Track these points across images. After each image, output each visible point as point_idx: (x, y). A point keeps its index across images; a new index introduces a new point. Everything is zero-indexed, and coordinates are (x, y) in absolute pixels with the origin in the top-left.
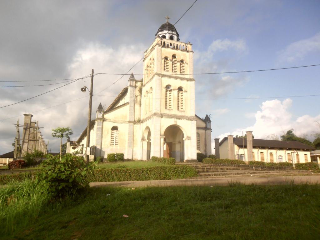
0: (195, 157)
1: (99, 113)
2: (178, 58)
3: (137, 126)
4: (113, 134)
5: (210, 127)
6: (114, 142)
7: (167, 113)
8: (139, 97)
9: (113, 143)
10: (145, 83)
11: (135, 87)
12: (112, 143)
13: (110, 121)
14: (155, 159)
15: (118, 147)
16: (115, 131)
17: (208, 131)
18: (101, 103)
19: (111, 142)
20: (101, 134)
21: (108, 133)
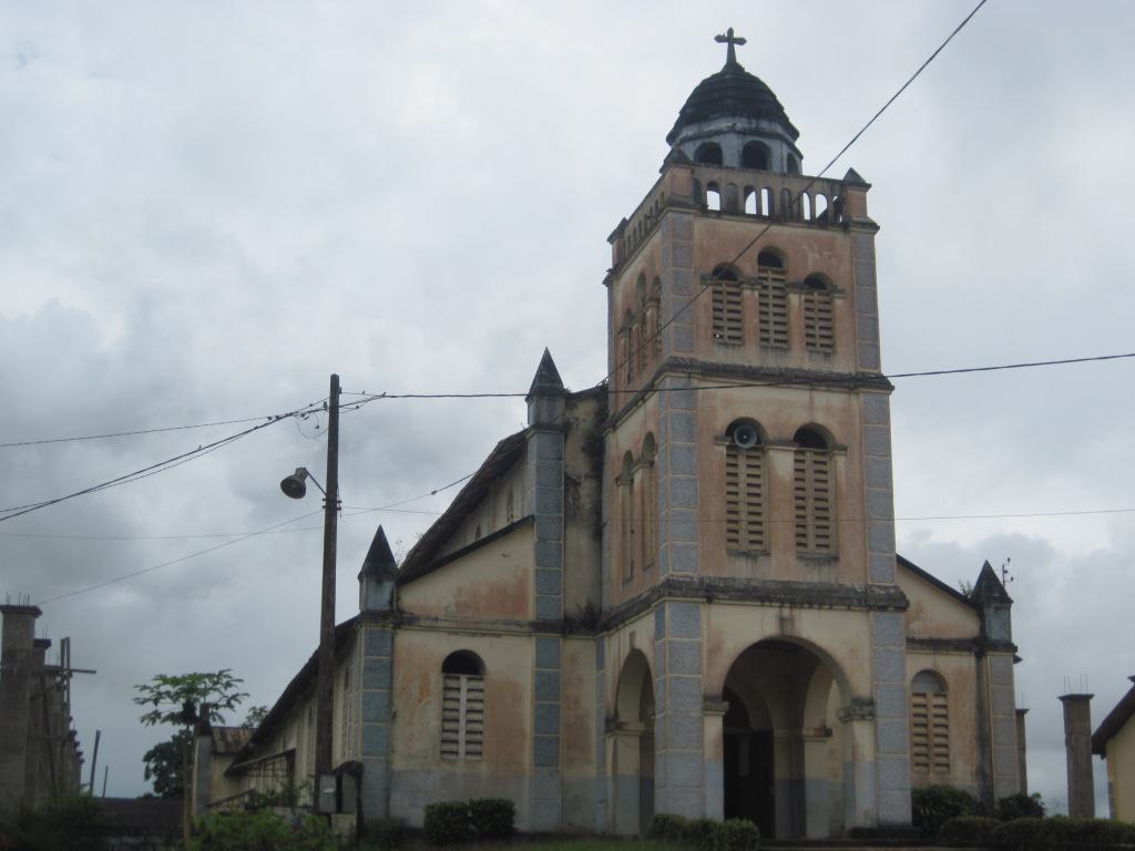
0: (899, 811)
1: (373, 584)
3: (577, 648)
4: (452, 694)
5: (1008, 630)
6: (462, 736)
7: (737, 576)
8: (586, 488)
9: (452, 747)
10: (622, 406)
11: (565, 429)
12: (447, 747)
13: (432, 624)
14: (665, 828)
15: (484, 768)
17: (993, 660)
18: (380, 532)
21: (424, 691)
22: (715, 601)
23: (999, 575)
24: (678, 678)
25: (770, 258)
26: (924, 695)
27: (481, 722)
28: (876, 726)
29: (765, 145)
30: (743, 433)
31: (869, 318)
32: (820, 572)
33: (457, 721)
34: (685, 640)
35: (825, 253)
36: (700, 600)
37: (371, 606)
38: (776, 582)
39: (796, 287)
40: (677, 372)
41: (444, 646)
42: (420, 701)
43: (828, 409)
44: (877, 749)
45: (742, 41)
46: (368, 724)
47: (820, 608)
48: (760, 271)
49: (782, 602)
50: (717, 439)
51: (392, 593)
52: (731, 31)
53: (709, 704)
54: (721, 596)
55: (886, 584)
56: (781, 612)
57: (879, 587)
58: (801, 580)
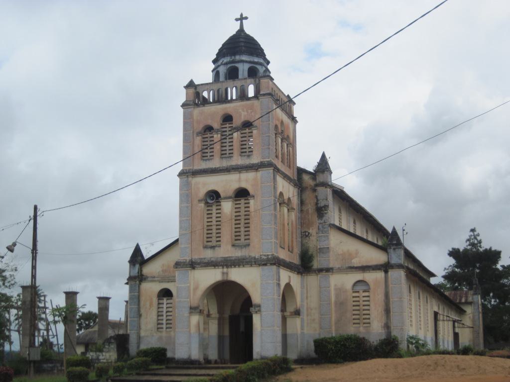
2: (237, 122)
4: (161, 306)
6: (164, 322)
7: (207, 257)
12: (159, 326)
13: (153, 279)
16: (165, 299)
19: (158, 324)
20: (137, 310)
23: (400, 233)
24: (180, 301)
25: (228, 118)
26: (358, 292)
27: (171, 316)
28: (261, 315)
30: (214, 196)
33: (162, 316)
34: (183, 285)
35: (249, 111)
36: (189, 269)
37: (132, 275)
39: (237, 129)
41: (157, 287)
42: (150, 309)
43: (247, 181)
44: (261, 326)
45: (246, 18)
47: (239, 267)
48: (222, 124)
50: (200, 201)
52: (242, 15)
53: (192, 310)
54: (198, 266)
58: (233, 255)
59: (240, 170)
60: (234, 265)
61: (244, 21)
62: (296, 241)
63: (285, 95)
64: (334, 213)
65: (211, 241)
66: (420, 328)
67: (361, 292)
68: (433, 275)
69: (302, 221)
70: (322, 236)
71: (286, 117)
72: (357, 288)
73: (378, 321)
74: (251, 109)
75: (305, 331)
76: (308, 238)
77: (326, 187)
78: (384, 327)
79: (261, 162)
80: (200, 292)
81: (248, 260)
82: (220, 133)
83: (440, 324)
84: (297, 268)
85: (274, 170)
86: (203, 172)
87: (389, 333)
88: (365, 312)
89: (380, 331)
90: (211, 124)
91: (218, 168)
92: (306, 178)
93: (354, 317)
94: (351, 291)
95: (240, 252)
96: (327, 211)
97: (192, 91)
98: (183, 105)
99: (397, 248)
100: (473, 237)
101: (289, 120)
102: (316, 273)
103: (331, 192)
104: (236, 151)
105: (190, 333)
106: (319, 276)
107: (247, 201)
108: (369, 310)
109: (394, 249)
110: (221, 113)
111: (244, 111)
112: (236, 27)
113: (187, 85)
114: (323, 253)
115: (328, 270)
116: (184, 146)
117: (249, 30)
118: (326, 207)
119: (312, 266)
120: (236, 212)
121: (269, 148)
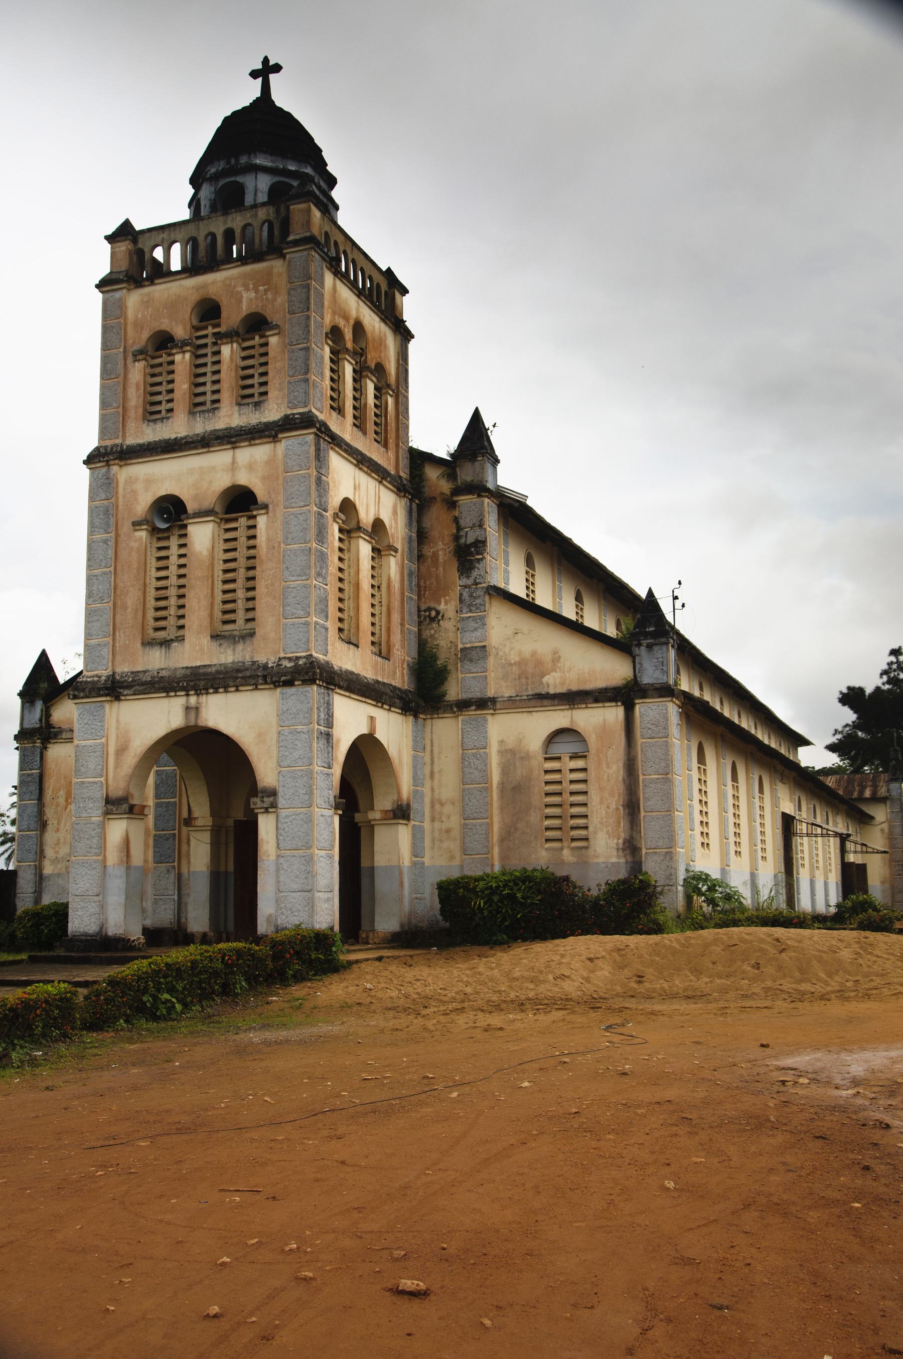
2: (231, 318)
7: (150, 668)
22: (123, 698)
24: (83, 783)
26: (559, 758)
29: (238, 182)
31: (301, 349)
32: (234, 650)
35: (261, 288)
37: (26, 726)
38: (187, 668)
40: (97, 462)
42: (66, 809)
43: (251, 467)
44: (278, 847)
45: (277, 68)
46: (21, 833)
47: (226, 692)
49: (187, 690)
50: (136, 524)
51: (42, 710)
53: (110, 807)
54: (125, 693)
55: (298, 655)
56: (187, 701)
57: (290, 659)
58: (215, 661)
59: (233, 440)
60: (212, 687)
61: (272, 77)
62: (402, 632)
63: (379, 269)
64: (507, 564)
65: (164, 629)
66: (738, 853)
67: (566, 758)
68: (800, 741)
69: (422, 584)
70: (470, 617)
71: (377, 319)
72: (556, 750)
73: (608, 833)
74: (264, 285)
75: (427, 861)
76: (434, 625)
77: (479, 496)
78: (624, 850)
79: (286, 418)
80: (131, 759)
81: (248, 673)
82: (188, 348)
83: (803, 846)
84: (400, 698)
85: (316, 434)
86: (145, 450)
87: (636, 867)
88: (575, 810)
89: (614, 860)
90: (168, 329)
91: (182, 439)
92: (432, 474)
93: (547, 823)
94: (541, 757)
95: (230, 652)
96: (482, 554)
97: (124, 246)
98: (102, 285)
99: (656, 644)
100: (895, 666)
101: (383, 325)
102: (454, 713)
103: (495, 508)
104: (227, 397)
105: (105, 866)
106: (460, 718)
107: (251, 523)
108: (585, 805)
109: (650, 647)
110: (194, 298)
111: (247, 289)
112: (251, 91)
113: (113, 233)
114: (471, 661)
115: (484, 703)
116: (103, 388)
117: (281, 98)
118: (480, 545)
119: (444, 695)
120: (226, 551)
121: (307, 381)
